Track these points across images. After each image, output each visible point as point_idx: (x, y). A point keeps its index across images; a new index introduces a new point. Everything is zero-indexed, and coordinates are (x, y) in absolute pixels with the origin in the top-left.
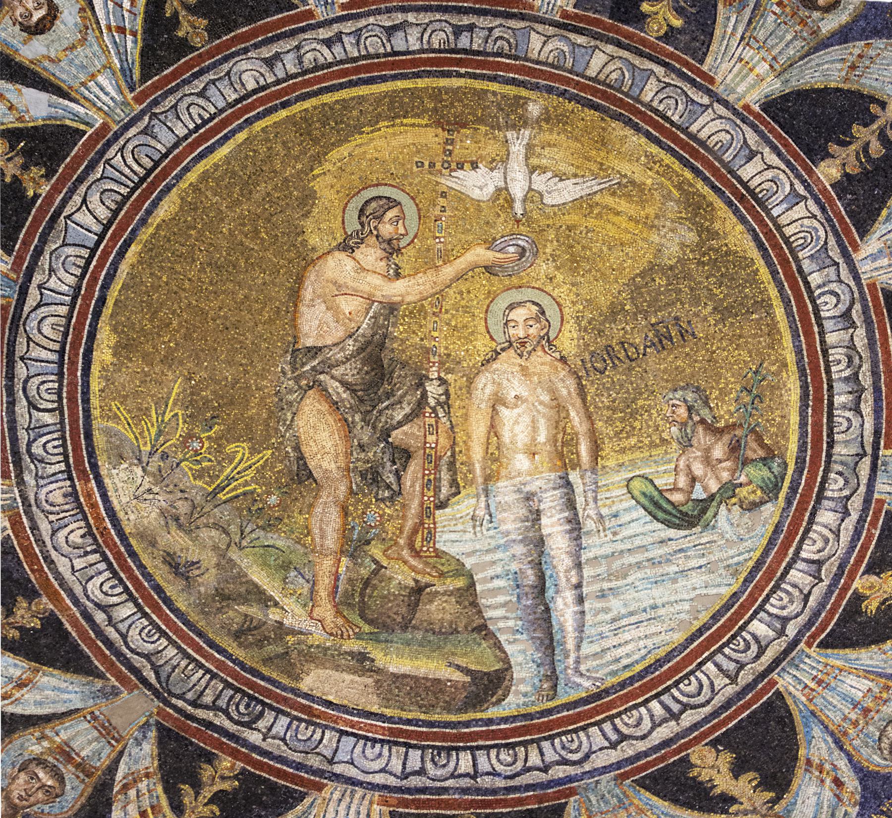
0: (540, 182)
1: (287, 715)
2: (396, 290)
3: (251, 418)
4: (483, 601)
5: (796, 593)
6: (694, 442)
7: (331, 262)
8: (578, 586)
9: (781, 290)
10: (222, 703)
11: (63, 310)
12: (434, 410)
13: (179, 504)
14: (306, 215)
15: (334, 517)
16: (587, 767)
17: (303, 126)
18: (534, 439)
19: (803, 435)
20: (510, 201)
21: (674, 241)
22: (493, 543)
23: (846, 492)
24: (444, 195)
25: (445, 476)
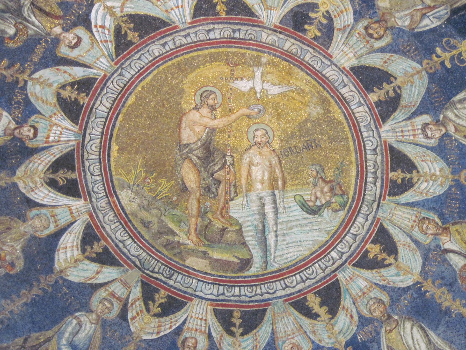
0: (266, 86)
1: (182, 274)
2: (215, 123)
3: (166, 170)
4: (245, 234)
5: (347, 245)
6: (318, 184)
7: (191, 114)
8: (276, 231)
9: (353, 136)
10: (161, 271)
11: (99, 141)
12: (229, 166)
13: (144, 201)
14: (181, 98)
15: (195, 203)
16: (275, 295)
17: (179, 67)
18: (263, 178)
19: (355, 189)
20: (256, 93)
21: (315, 111)
22: (249, 214)
23: (368, 213)
24: (231, 89)
25: (233, 190)
